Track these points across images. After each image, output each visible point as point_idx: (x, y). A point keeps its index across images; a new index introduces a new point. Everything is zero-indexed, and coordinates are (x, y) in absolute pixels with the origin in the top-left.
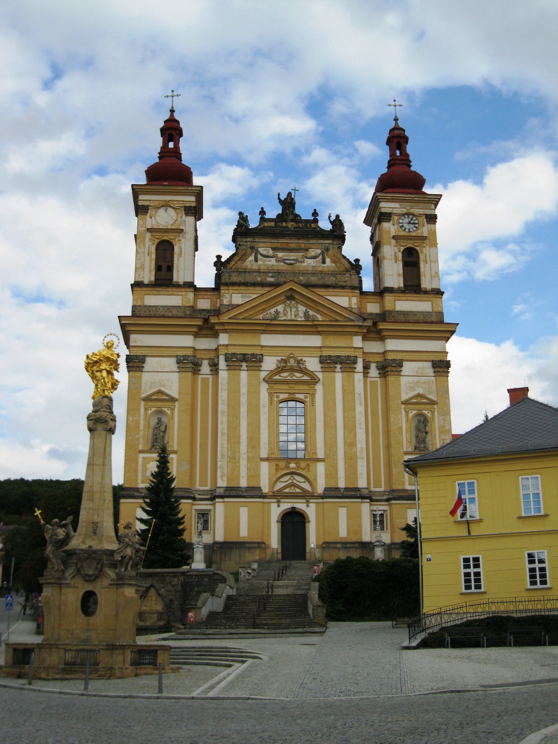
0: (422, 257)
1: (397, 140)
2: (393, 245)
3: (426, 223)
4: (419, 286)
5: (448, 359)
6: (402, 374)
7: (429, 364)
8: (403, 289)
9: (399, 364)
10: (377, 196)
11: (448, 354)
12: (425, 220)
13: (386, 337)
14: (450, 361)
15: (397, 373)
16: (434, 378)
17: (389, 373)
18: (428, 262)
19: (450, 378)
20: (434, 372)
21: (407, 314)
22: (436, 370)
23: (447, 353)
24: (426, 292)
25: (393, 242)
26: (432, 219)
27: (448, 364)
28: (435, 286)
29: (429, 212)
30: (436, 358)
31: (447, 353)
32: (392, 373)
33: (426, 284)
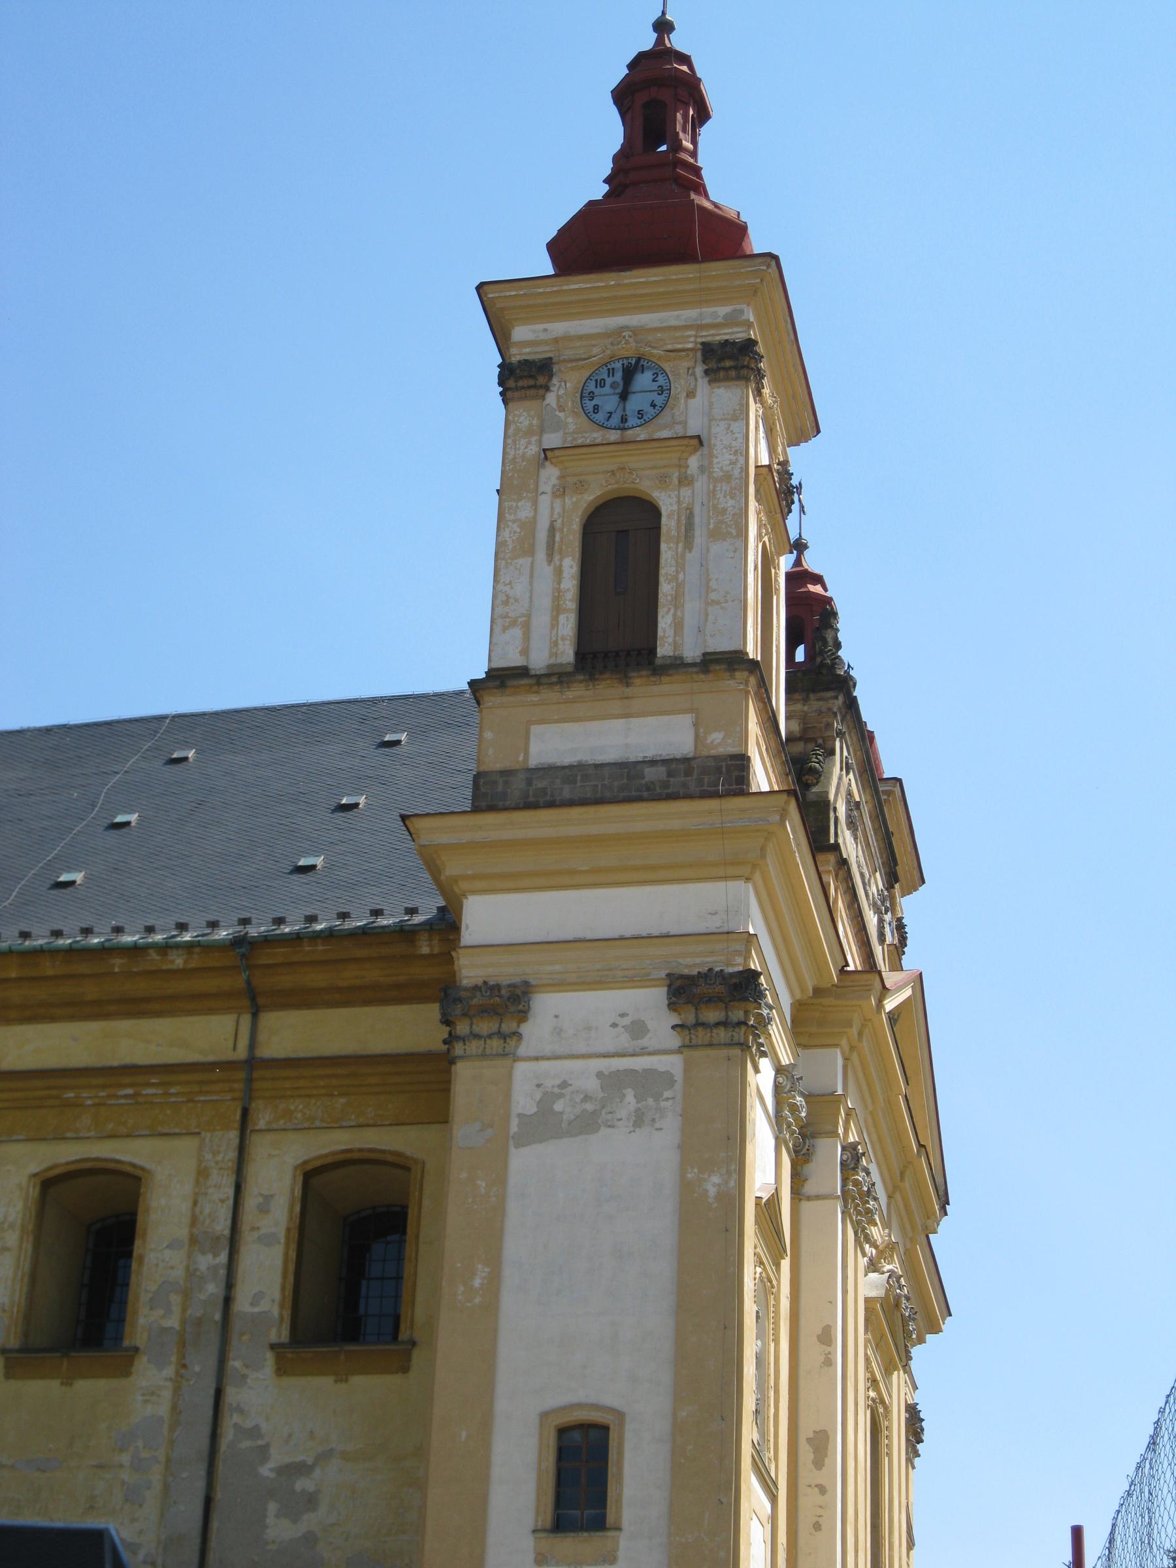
21: (585, 778)
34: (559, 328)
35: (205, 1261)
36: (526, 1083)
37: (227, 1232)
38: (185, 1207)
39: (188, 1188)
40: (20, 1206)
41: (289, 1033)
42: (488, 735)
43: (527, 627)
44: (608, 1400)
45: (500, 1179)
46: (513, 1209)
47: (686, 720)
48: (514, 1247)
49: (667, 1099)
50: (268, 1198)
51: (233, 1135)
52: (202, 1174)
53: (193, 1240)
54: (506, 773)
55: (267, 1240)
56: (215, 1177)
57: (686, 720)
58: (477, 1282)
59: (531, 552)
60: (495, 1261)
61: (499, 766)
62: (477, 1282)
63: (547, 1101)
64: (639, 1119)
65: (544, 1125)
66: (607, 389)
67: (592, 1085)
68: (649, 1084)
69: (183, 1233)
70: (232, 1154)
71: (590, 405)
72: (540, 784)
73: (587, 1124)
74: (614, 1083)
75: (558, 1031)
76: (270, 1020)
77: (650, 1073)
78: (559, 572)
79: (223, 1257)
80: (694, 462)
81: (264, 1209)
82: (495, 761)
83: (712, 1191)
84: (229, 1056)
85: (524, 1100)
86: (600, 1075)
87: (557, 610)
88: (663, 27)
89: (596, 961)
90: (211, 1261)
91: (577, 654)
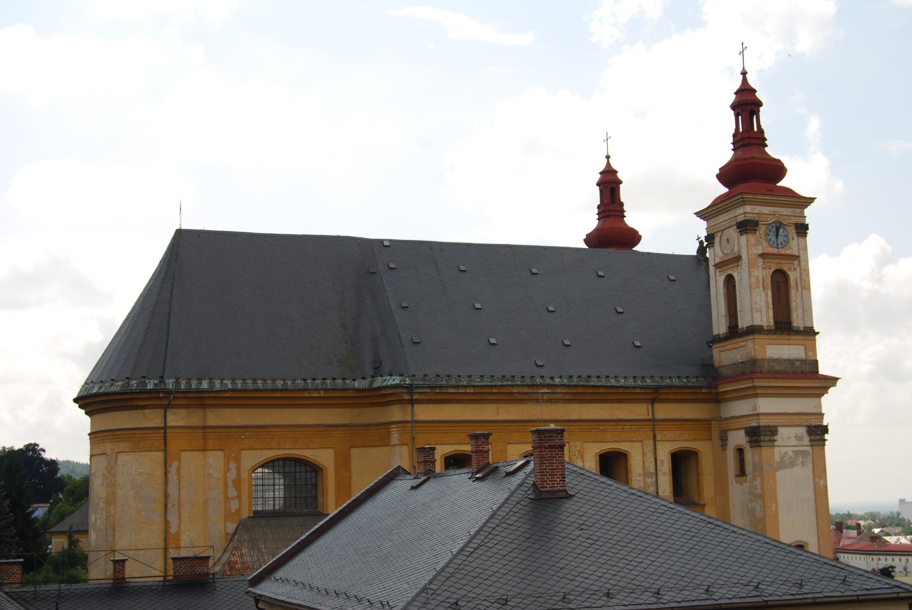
1: (746, 104)
3: (795, 235)
4: (789, 323)
5: (825, 423)
6: (776, 444)
7: (802, 431)
9: (773, 431)
12: (794, 231)
15: (770, 444)
16: (809, 449)
17: (762, 444)
18: (799, 289)
19: (828, 447)
20: (811, 440)
22: (813, 438)
24: (798, 332)
25: (760, 261)
26: (802, 229)
27: (825, 430)
28: (808, 325)
29: (800, 221)
30: (814, 422)
32: (765, 444)
33: (797, 322)
34: (758, 209)
35: (650, 480)
36: (777, 452)
38: (641, 463)
39: (641, 458)
41: (663, 411)
44: (804, 539)
45: (775, 481)
47: (803, 347)
51: (651, 442)
52: (644, 454)
53: (645, 474)
54: (763, 360)
55: (664, 474)
57: (803, 347)
59: (759, 287)
60: (776, 503)
63: (782, 458)
64: (803, 464)
65: (782, 465)
67: (791, 454)
68: (804, 454)
69: (641, 471)
70: (652, 448)
73: (792, 465)
74: (797, 453)
75: (782, 438)
76: (657, 406)
77: (804, 451)
78: (766, 295)
79: (654, 479)
80: (796, 262)
81: (662, 464)
82: (759, 356)
84: (647, 417)
87: (768, 308)
88: (744, 73)
89: (792, 419)
90: (650, 480)
91: (775, 322)
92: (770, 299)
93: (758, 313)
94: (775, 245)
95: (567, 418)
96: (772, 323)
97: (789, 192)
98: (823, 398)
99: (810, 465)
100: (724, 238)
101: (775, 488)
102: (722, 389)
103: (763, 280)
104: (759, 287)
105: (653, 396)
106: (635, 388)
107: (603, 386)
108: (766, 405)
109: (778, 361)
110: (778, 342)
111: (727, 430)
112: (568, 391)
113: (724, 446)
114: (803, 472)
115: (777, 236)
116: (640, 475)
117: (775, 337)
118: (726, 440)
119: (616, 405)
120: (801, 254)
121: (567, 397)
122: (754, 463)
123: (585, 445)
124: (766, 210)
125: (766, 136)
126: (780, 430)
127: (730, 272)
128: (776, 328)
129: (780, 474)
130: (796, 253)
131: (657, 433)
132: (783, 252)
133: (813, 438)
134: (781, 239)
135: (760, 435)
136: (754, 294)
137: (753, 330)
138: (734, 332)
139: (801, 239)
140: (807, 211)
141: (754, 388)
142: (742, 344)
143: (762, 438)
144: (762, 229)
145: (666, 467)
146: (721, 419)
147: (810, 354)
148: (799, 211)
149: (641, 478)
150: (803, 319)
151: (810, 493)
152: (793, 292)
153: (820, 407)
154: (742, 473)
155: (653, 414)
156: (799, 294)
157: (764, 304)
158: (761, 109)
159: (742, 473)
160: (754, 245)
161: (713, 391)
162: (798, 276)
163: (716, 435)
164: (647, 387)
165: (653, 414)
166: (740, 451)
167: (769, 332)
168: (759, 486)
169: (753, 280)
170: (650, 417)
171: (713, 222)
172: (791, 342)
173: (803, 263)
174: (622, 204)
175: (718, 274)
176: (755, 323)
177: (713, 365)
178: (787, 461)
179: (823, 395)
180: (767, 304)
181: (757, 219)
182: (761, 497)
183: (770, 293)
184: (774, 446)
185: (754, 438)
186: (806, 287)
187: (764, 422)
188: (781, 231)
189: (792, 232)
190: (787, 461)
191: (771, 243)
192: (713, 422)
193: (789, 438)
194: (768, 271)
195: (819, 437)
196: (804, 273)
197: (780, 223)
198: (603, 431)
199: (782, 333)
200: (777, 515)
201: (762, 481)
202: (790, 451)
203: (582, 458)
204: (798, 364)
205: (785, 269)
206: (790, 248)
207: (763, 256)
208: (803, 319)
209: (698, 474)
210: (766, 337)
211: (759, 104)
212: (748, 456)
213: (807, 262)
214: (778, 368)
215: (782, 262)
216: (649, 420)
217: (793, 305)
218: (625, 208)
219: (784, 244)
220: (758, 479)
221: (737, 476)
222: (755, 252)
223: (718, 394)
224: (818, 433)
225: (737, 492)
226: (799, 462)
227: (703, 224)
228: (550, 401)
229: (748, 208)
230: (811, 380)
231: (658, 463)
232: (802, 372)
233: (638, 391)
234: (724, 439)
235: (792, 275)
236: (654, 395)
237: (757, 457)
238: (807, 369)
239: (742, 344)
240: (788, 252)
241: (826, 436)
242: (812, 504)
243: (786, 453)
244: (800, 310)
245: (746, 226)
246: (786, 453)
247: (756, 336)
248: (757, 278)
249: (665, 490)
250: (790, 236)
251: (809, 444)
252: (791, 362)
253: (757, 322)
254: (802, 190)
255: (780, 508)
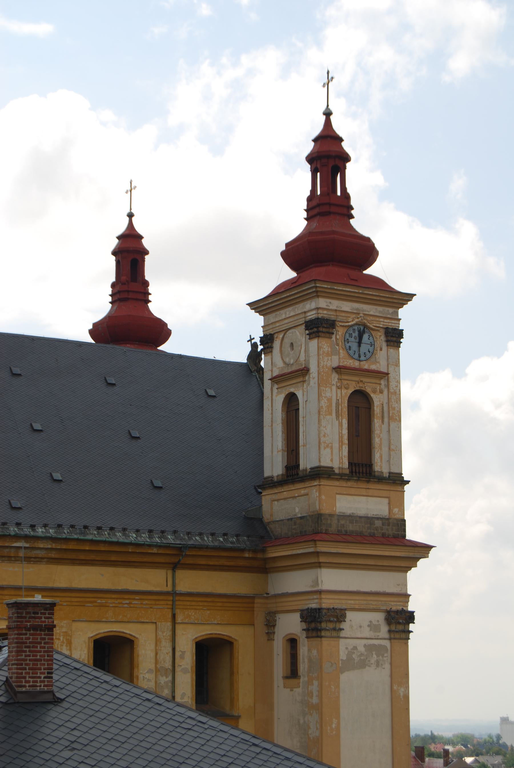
0: (377, 410)
2: (334, 388)
3: (384, 345)
4: (370, 465)
5: (410, 608)
6: (342, 634)
8: (347, 472)
9: (339, 616)
10: (316, 287)
11: (411, 598)
12: (383, 338)
13: (322, 564)
14: (413, 612)
15: (334, 634)
17: (323, 633)
18: (386, 420)
20: (390, 631)
22: (393, 628)
23: (410, 595)
24: (380, 479)
25: (335, 377)
26: (394, 337)
27: (410, 617)
28: (394, 470)
29: (391, 324)
30: (396, 606)
31: (410, 595)
32: (328, 634)
33: (380, 466)
34: (335, 304)
37: (170, 667)
38: (153, 655)
39: (153, 647)
40: (86, 652)
41: (188, 581)
42: (323, 497)
43: (332, 448)
45: (338, 686)
46: (341, 695)
47: (386, 501)
48: (344, 712)
49: (386, 657)
50: (183, 653)
51: (169, 624)
52: (157, 641)
53: (157, 670)
54: (331, 515)
55: (185, 671)
56: (164, 643)
57: (386, 501)
58: (334, 726)
59: (331, 414)
60: (338, 717)
61: (327, 512)
62: (334, 726)
64: (378, 664)
65: (350, 664)
66: (353, 339)
67: (361, 649)
68: (379, 650)
69: (153, 666)
70: (169, 633)
71: (348, 345)
72: (342, 522)
73: (363, 664)
74: (370, 648)
75: (351, 627)
76: (180, 574)
77: (380, 646)
78: (341, 425)
79: (170, 678)
80: (383, 382)
81: (182, 657)
82: (326, 510)
83: (402, 694)
84: (165, 589)
85: (343, 655)
86: (365, 646)
87: (341, 442)
88: (328, 114)
90: (164, 680)
91: (350, 464)
92: (345, 432)
93: (328, 450)
94: (356, 356)
95: (50, 585)
96: (346, 465)
97: (379, 284)
98: (412, 574)
99: (387, 666)
100: (287, 341)
101: (338, 697)
102: (274, 553)
103: (337, 404)
104: (331, 414)
105: (175, 560)
106: (150, 546)
107: (105, 542)
108: (333, 580)
109: (352, 518)
110: (353, 491)
111: (275, 613)
112: (54, 546)
113: (270, 635)
114: (378, 676)
115: (360, 343)
116: (150, 671)
117: (349, 484)
118: (274, 626)
119: (122, 570)
120: (391, 370)
121: (53, 555)
122: (310, 660)
123: (75, 625)
124: (346, 306)
125: (353, 203)
126: (350, 615)
127: (292, 390)
128: (351, 472)
129: (345, 678)
130: (383, 369)
131: (178, 611)
132: (366, 367)
133: (393, 628)
134: (364, 348)
135: (320, 621)
136: (323, 423)
137: (320, 473)
138: (293, 474)
139: (392, 351)
140: (402, 312)
141: (317, 554)
142: (303, 492)
143: (324, 625)
144: (340, 332)
145: (187, 660)
146: (268, 596)
147: (396, 510)
148: (391, 310)
149: (152, 676)
150: (389, 461)
151: (385, 705)
152: (377, 423)
153: (406, 585)
154: (293, 673)
155: (174, 585)
156: (385, 427)
157: (337, 437)
158: (348, 165)
159: (293, 673)
160: (328, 355)
161: (260, 556)
162: (386, 401)
163: (260, 619)
164: (167, 546)
165: (174, 585)
166: (292, 643)
167: (341, 477)
168: (315, 693)
169: (324, 403)
170: (170, 589)
171: (272, 318)
172: (370, 492)
173: (392, 384)
174: (146, 284)
175: (275, 391)
176: (323, 464)
177: (260, 520)
178: (356, 659)
179: (410, 568)
180: (341, 437)
181: (333, 318)
182: (318, 708)
183: (345, 422)
184: (339, 637)
185: (313, 625)
186: (395, 417)
187: (327, 603)
188: (365, 337)
189: (380, 339)
190: (356, 659)
191: (351, 352)
192: (257, 600)
193: (361, 626)
194: (344, 391)
195: (400, 627)
196: (393, 398)
197: (365, 326)
198: (101, 606)
199: (358, 480)
200: (338, 735)
201: (321, 685)
202: (361, 645)
203: (69, 643)
204: (378, 523)
205: (368, 390)
206: (376, 362)
207: (339, 370)
208: (389, 461)
209: (232, 673)
210: (337, 483)
211: (346, 158)
212: (303, 650)
213: (399, 382)
214: (351, 527)
215: (364, 380)
216: (167, 593)
217: (376, 441)
218: (151, 289)
219: (368, 355)
220: (316, 683)
221: (286, 678)
222: (329, 364)
223: (266, 560)
224: (400, 621)
225: (286, 700)
226: (373, 661)
227: (259, 320)
228: (28, 559)
229: (322, 302)
230: (394, 547)
231: (177, 654)
232: (383, 535)
233: (155, 550)
234: (270, 625)
235: (377, 400)
236: (177, 558)
237: (315, 652)
238: (390, 531)
239: (303, 492)
240: (373, 367)
241: (411, 627)
242: (387, 721)
243: (355, 648)
244: (385, 449)
245: (318, 327)
246: (355, 648)
247: (324, 482)
248: (330, 400)
249: (183, 695)
250: (377, 345)
251: (387, 636)
252: (369, 520)
253: (326, 462)
254: (399, 285)
255: (342, 724)
